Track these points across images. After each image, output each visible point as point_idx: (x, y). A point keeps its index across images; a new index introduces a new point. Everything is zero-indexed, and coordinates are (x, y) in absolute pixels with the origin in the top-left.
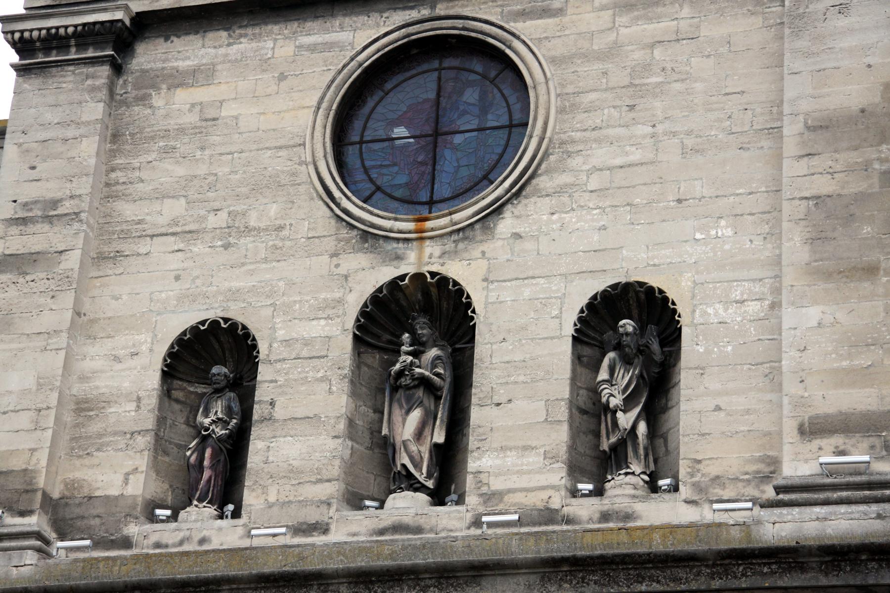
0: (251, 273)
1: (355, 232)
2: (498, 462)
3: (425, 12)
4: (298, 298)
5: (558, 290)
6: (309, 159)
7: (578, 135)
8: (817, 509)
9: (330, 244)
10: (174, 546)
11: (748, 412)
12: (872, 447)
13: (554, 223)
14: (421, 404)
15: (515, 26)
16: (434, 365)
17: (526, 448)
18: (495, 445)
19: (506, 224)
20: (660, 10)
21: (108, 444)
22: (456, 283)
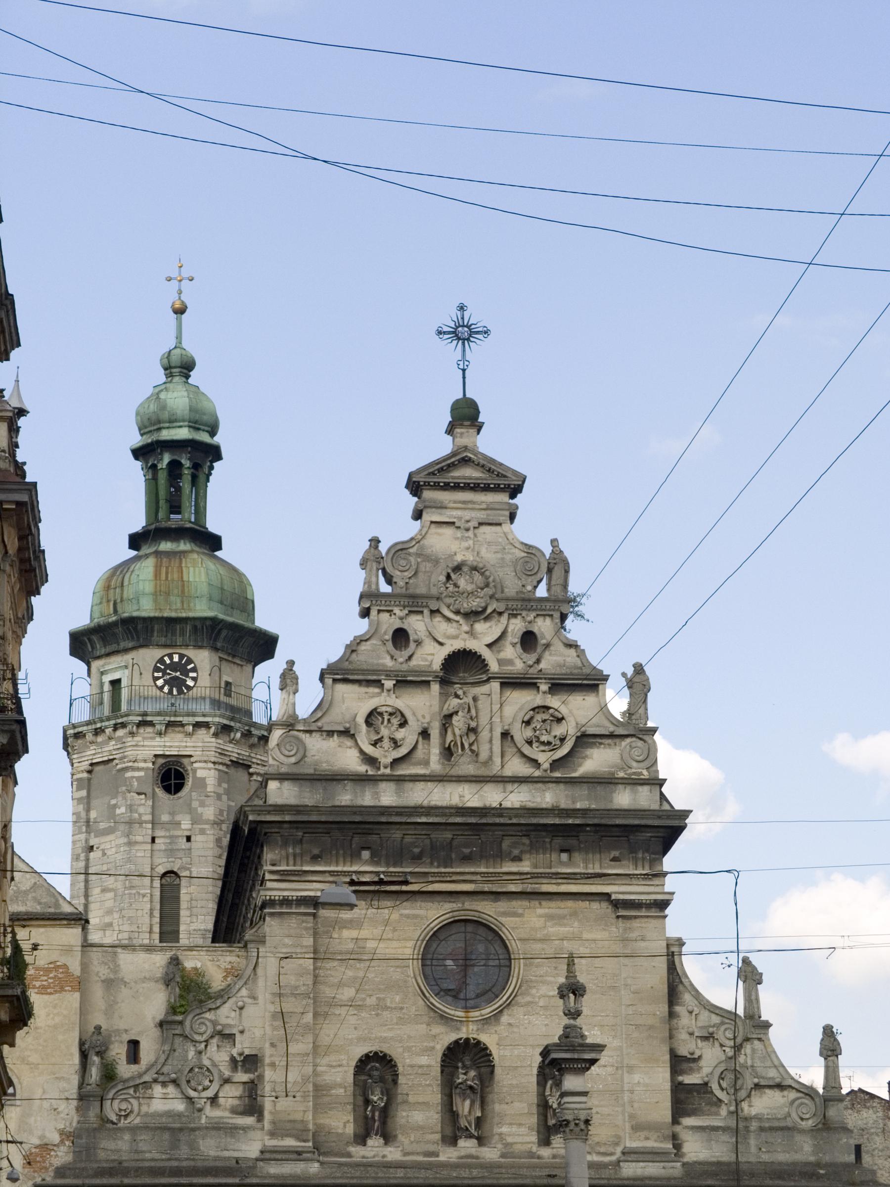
0: (391, 1030)
1: (437, 1015)
2: (509, 1130)
3: (460, 905)
4: (414, 1044)
5: (529, 1053)
6: (412, 975)
7: (534, 978)
8: (642, 1164)
9: (426, 1019)
10: (371, 1158)
11: (609, 1115)
12: (659, 1137)
13: (526, 1020)
14: (469, 1097)
15: (503, 919)
16: (473, 1080)
17: (520, 1125)
18: (508, 1122)
19: (505, 1019)
20: (565, 921)
21: (333, 1108)
22: (484, 1044)
